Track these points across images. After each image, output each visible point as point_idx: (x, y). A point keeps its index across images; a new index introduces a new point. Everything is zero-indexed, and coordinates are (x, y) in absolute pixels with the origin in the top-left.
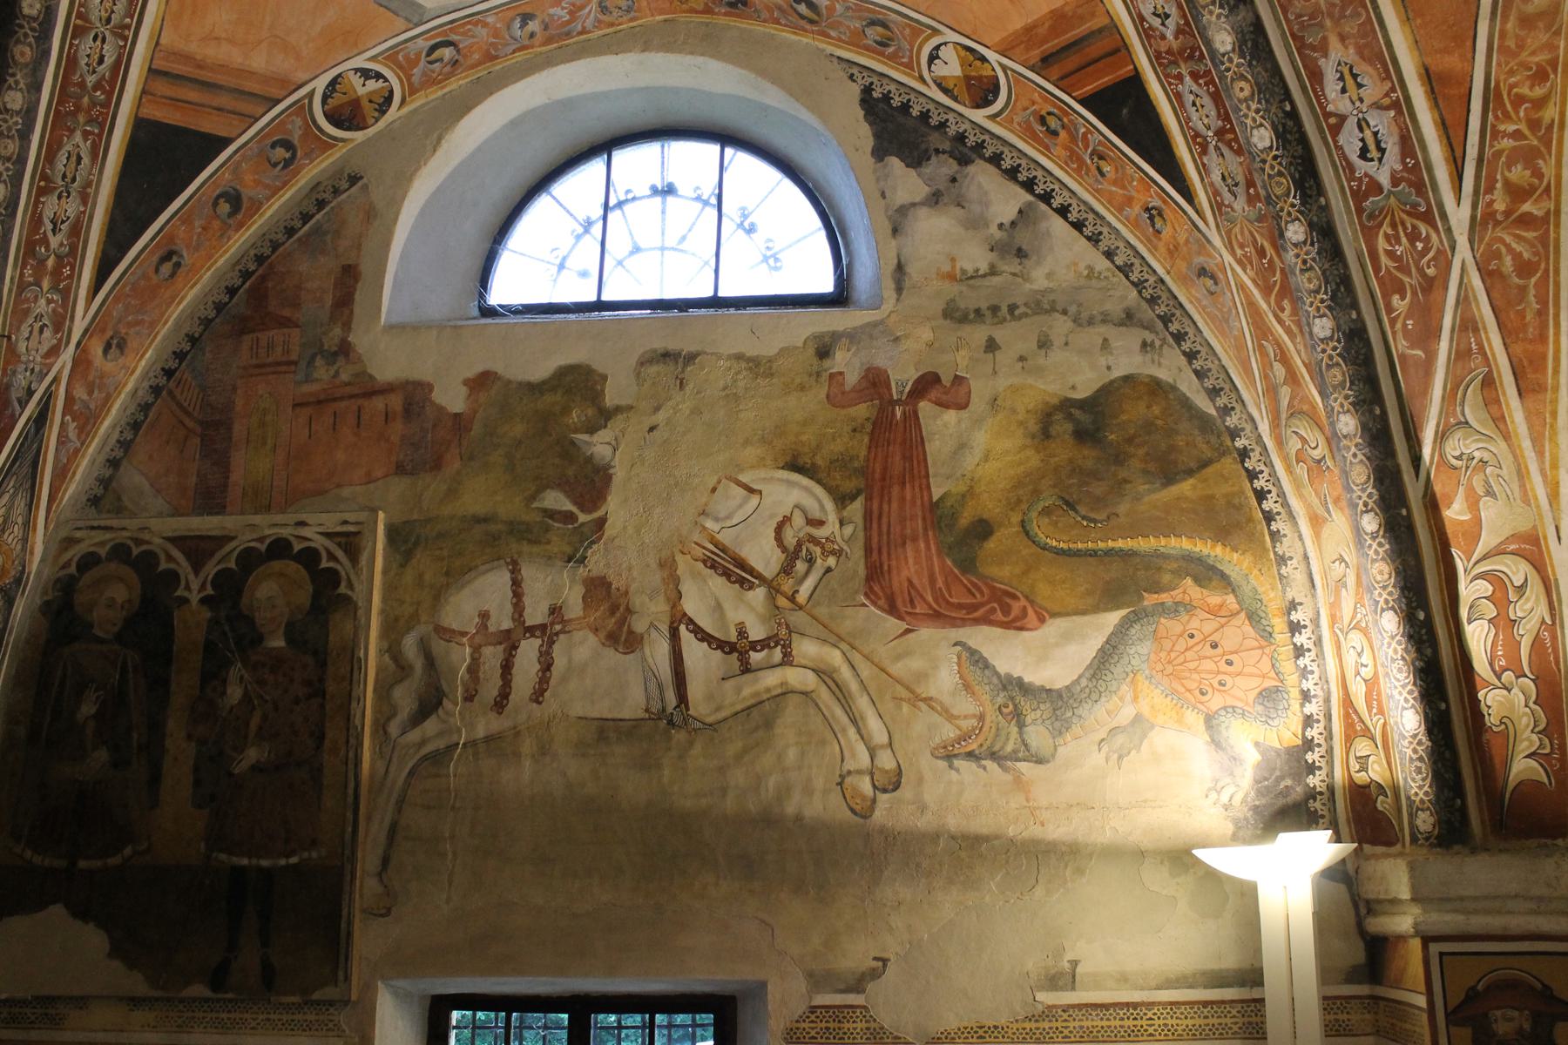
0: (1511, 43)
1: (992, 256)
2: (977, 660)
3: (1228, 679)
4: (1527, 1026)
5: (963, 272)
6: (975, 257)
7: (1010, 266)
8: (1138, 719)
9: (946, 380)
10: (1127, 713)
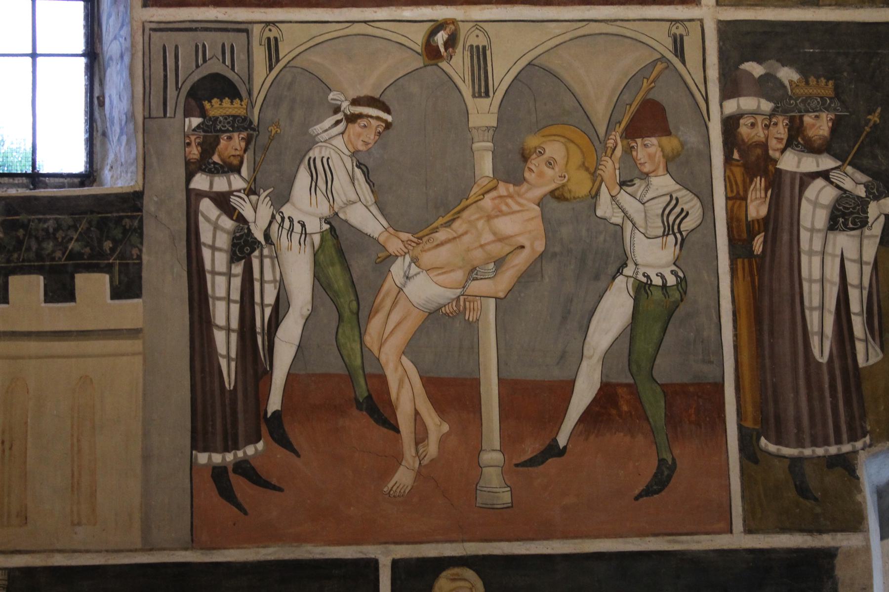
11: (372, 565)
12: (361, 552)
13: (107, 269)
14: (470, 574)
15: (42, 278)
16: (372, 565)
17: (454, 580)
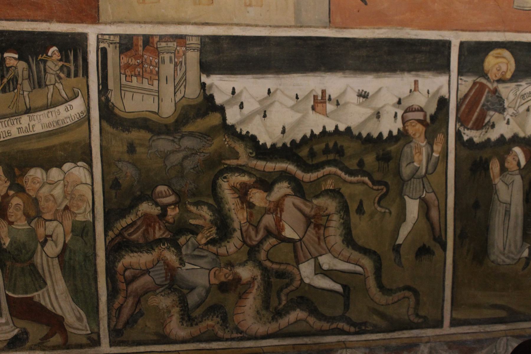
11: (446, 45)
12: (440, 36)
14: (506, 53)
16: (446, 45)
17: (497, 57)
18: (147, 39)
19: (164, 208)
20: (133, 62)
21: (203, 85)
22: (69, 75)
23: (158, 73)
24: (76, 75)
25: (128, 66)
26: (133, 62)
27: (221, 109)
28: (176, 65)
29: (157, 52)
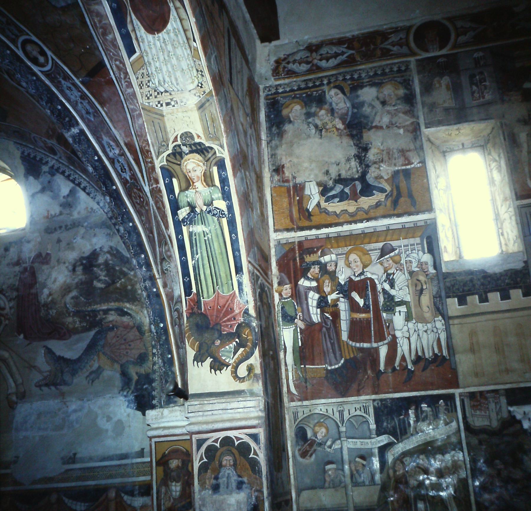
0: (139, 134)
1: (61, 208)
2: (49, 351)
3: (129, 351)
4: (180, 465)
5: (51, 215)
6: (56, 209)
7: (67, 211)
8: (99, 367)
9: (44, 255)
10: (96, 365)
13: (520, 287)
15: (498, 293)
18: (481, 393)
19: (499, 471)
20: (476, 403)
21: (509, 412)
22: (449, 412)
23: (488, 408)
24: (452, 412)
25: (474, 406)
26: (476, 403)
27: (520, 422)
28: (496, 403)
29: (486, 399)
